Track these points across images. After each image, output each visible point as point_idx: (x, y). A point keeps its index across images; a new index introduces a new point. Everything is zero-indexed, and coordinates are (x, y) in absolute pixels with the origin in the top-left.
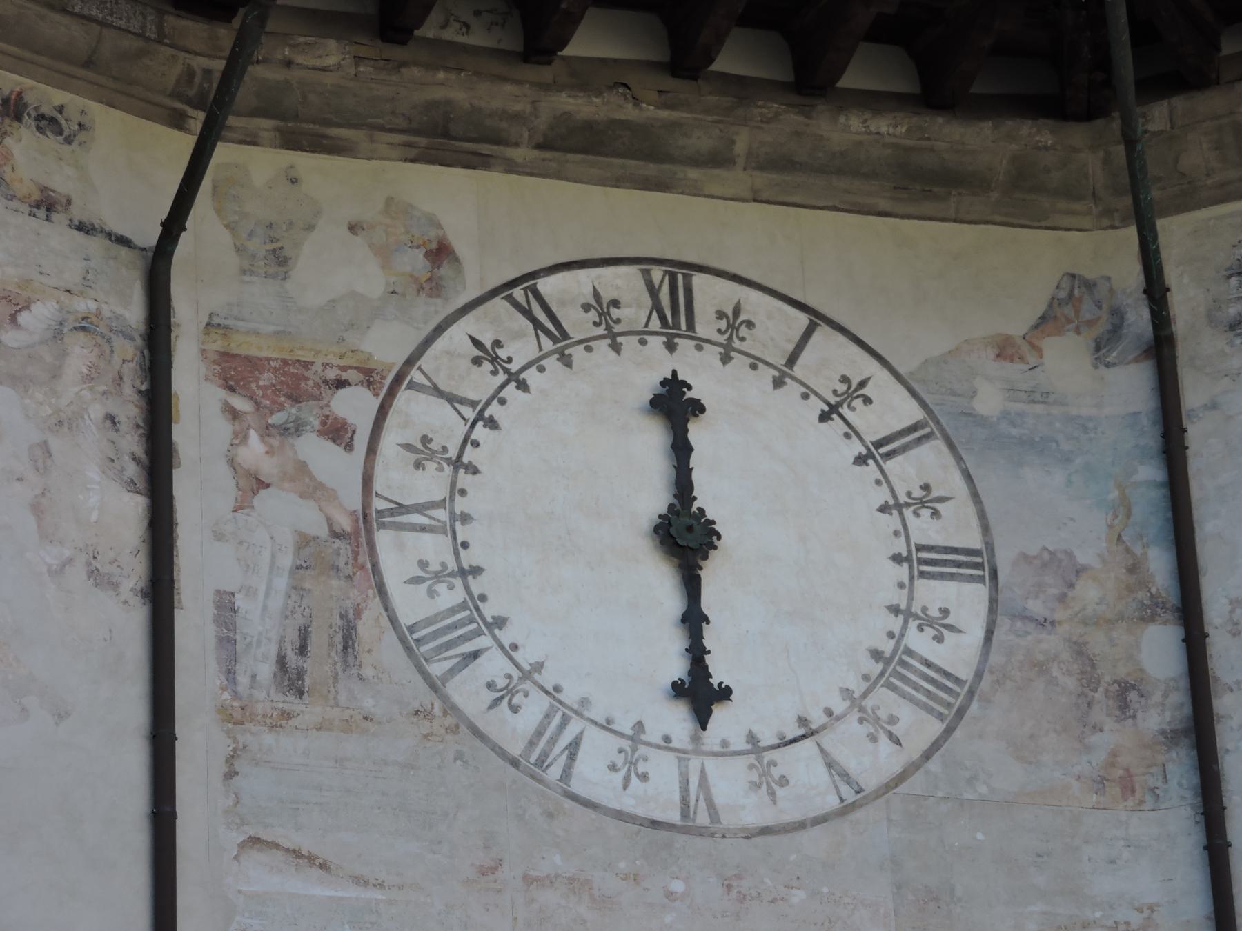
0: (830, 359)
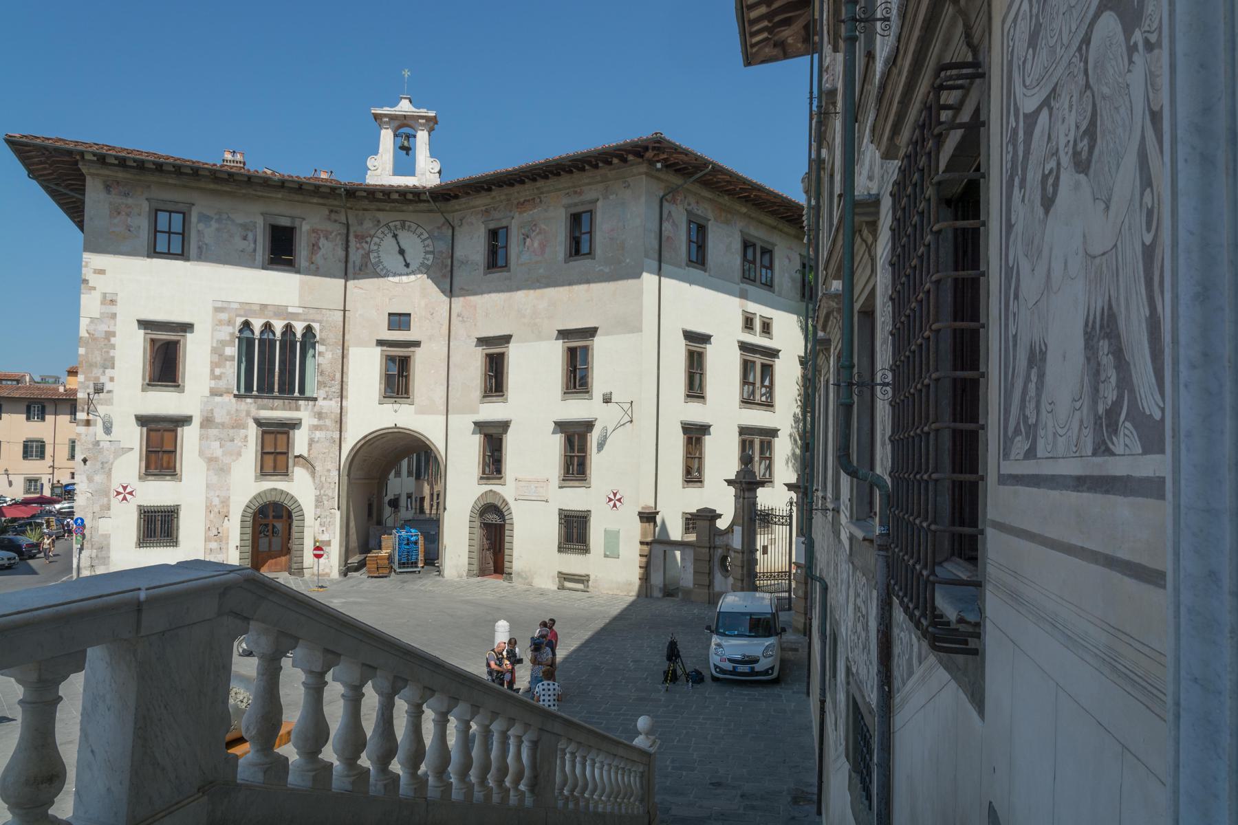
0: (420, 230)
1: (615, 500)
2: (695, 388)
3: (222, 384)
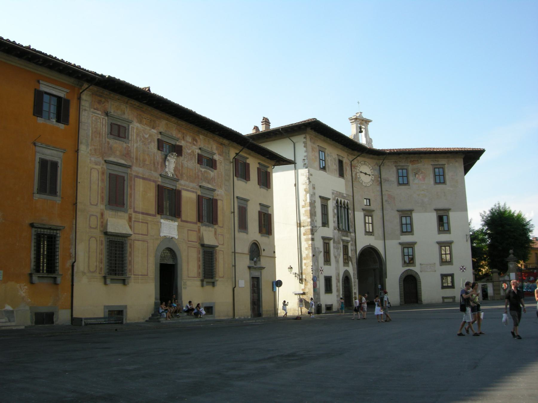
0: (370, 166)
1: (463, 269)
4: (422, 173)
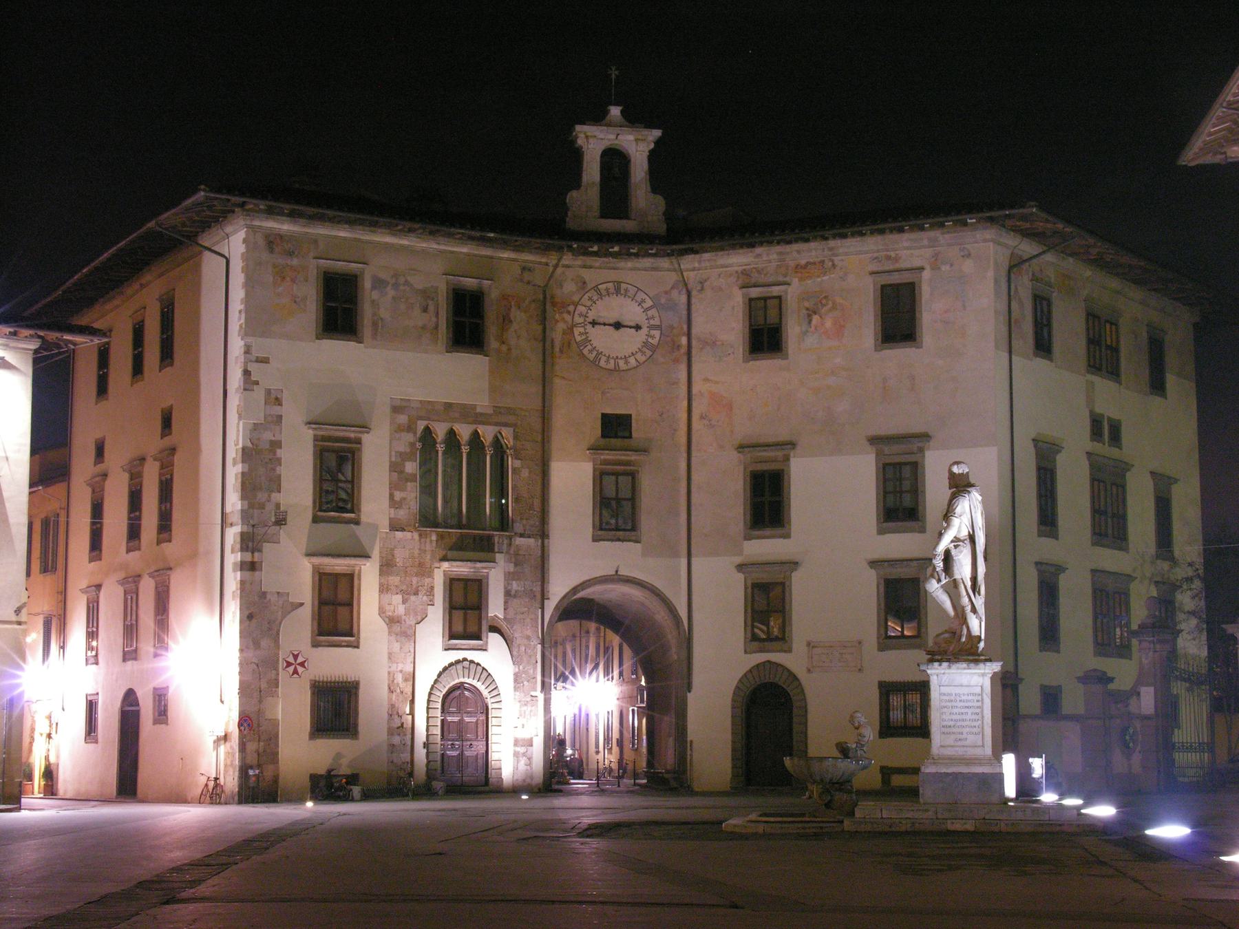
0: (641, 296)
2: (1048, 520)
3: (402, 514)
4: (834, 308)
